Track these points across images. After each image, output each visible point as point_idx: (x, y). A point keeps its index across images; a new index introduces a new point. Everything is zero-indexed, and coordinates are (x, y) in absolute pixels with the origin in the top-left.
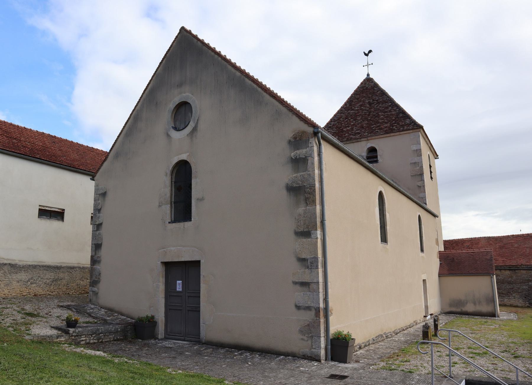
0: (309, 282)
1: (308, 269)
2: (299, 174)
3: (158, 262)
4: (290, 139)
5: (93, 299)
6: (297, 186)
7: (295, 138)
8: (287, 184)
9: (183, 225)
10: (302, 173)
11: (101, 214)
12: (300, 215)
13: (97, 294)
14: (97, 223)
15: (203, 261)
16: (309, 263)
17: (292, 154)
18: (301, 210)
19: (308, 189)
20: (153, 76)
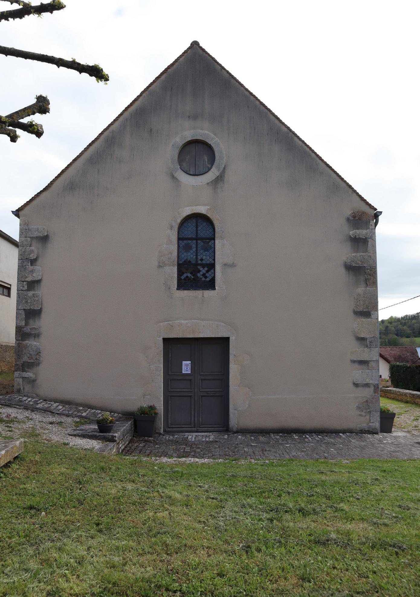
0: (368, 360)
1: (367, 348)
2: (358, 254)
3: (158, 339)
4: (348, 216)
5: (24, 389)
6: (356, 265)
7: (354, 217)
8: (346, 262)
9: (202, 294)
10: (362, 254)
11: (37, 268)
12: (359, 295)
13: (34, 381)
14: (30, 279)
15: (234, 338)
16: (368, 343)
17: (351, 233)
18: (361, 290)
19: (368, 271)
20: (142, 93)
